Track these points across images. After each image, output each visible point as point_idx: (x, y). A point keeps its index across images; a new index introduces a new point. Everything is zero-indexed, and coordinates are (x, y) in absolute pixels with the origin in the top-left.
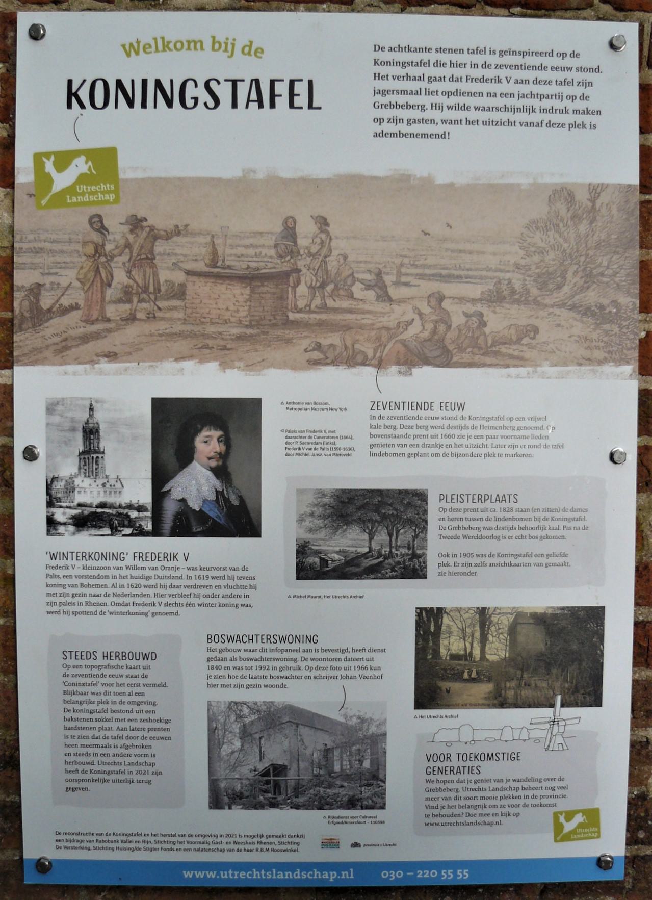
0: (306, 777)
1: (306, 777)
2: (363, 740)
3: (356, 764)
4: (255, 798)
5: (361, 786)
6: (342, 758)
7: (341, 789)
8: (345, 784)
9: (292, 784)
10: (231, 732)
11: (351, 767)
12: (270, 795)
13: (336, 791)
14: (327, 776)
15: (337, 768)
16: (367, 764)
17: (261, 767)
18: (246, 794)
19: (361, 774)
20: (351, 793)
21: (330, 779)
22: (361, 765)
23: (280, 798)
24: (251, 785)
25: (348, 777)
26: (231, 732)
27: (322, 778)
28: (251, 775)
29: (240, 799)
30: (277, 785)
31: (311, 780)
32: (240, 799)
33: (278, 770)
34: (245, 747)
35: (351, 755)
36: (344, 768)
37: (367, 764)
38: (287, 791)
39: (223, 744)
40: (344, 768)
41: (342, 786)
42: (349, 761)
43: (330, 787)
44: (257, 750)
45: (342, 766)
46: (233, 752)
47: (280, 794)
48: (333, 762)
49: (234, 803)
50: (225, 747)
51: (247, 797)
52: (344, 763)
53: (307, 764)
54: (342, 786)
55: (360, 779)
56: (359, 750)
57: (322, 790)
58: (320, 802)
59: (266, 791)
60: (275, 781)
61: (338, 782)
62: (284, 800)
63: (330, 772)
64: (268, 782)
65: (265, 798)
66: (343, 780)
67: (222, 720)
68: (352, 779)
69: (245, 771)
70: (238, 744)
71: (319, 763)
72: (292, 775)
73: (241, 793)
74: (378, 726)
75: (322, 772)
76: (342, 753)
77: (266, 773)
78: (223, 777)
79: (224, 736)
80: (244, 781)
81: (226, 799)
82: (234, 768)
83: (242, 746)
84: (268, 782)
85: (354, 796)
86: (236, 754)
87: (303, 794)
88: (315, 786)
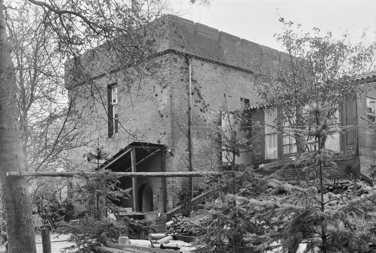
0: (206, 170)
1: (206, 170)
2: (325, 91)
3: (311, 143)
4: (98, 217)
5: (322, 191)
6: (280, 129)
7: (279, 199)
8: (288, 186)
9: (177, 184)
10: (48, 75)
11: (301, 150)
12: (129, 211)
13: (270, 201)
14: (250, 169)
15: (271, 151)
16: (333, 143)
17: (111, 150)
18: (80, 208)
19: (320, 165)
20: (301, 207)
21: (257, 176)
22: (322, 145)
23: (150, 217)
24: (91, 189)
25: (294, 172)
26: (48, 75)
27: (239, 174)
28: (89, 167)
29: (67, 219)
30: (144, 189)
31: (215, 179)
32: (67, 219)
33: (148, 155)
34: (79, 106)
35: (300, 123)
36: (286, 151)
37: (333, 143)
38: (165, 202)
39: (33, 99)
40: (286, 151)
41: (281, 192)
42: (297, 136)
43: (257, 191)
44: (102, 111)
45: (281, 146)
46: (52, 118)
47: (151, 208)
48: (263, 137)
49: (55, 228)
50: (36, 105)
51: (82, 215)
52: (286, 141)
53: (207, 143)
54: (281, 192)
55: (320, 175)
56: (317, 112)
57: (239, 199)
58: (234, 226)
59: (122, 202)
60: (139, 178)
61: (274, 183)
62: (161, 221)
63: (257, 160)
64: (125, 182)
65: (119, 218)
66: (284, 177)
67: (30, 49)
68: (303, 176)
69: (78, 158)
70: (62, 100)
71: (233, 141)
72: (176, 166)
73: (70, 207)
74: (357, 61)
75: (239, 161)
76: (280, 118)
77: (121, 163)
78: (32, 171)
79: (33, 83)
80: (75, 181)
81: (38, 221)
82: (55, 150)
83: (72, 103)
84: (125, 182)
85: (307, 213)
86: (59, 122)
87: (198, 208)
88: (226, 190)
